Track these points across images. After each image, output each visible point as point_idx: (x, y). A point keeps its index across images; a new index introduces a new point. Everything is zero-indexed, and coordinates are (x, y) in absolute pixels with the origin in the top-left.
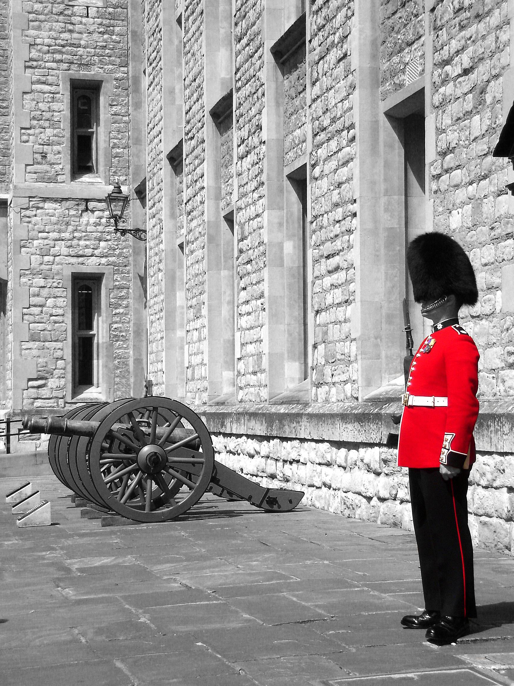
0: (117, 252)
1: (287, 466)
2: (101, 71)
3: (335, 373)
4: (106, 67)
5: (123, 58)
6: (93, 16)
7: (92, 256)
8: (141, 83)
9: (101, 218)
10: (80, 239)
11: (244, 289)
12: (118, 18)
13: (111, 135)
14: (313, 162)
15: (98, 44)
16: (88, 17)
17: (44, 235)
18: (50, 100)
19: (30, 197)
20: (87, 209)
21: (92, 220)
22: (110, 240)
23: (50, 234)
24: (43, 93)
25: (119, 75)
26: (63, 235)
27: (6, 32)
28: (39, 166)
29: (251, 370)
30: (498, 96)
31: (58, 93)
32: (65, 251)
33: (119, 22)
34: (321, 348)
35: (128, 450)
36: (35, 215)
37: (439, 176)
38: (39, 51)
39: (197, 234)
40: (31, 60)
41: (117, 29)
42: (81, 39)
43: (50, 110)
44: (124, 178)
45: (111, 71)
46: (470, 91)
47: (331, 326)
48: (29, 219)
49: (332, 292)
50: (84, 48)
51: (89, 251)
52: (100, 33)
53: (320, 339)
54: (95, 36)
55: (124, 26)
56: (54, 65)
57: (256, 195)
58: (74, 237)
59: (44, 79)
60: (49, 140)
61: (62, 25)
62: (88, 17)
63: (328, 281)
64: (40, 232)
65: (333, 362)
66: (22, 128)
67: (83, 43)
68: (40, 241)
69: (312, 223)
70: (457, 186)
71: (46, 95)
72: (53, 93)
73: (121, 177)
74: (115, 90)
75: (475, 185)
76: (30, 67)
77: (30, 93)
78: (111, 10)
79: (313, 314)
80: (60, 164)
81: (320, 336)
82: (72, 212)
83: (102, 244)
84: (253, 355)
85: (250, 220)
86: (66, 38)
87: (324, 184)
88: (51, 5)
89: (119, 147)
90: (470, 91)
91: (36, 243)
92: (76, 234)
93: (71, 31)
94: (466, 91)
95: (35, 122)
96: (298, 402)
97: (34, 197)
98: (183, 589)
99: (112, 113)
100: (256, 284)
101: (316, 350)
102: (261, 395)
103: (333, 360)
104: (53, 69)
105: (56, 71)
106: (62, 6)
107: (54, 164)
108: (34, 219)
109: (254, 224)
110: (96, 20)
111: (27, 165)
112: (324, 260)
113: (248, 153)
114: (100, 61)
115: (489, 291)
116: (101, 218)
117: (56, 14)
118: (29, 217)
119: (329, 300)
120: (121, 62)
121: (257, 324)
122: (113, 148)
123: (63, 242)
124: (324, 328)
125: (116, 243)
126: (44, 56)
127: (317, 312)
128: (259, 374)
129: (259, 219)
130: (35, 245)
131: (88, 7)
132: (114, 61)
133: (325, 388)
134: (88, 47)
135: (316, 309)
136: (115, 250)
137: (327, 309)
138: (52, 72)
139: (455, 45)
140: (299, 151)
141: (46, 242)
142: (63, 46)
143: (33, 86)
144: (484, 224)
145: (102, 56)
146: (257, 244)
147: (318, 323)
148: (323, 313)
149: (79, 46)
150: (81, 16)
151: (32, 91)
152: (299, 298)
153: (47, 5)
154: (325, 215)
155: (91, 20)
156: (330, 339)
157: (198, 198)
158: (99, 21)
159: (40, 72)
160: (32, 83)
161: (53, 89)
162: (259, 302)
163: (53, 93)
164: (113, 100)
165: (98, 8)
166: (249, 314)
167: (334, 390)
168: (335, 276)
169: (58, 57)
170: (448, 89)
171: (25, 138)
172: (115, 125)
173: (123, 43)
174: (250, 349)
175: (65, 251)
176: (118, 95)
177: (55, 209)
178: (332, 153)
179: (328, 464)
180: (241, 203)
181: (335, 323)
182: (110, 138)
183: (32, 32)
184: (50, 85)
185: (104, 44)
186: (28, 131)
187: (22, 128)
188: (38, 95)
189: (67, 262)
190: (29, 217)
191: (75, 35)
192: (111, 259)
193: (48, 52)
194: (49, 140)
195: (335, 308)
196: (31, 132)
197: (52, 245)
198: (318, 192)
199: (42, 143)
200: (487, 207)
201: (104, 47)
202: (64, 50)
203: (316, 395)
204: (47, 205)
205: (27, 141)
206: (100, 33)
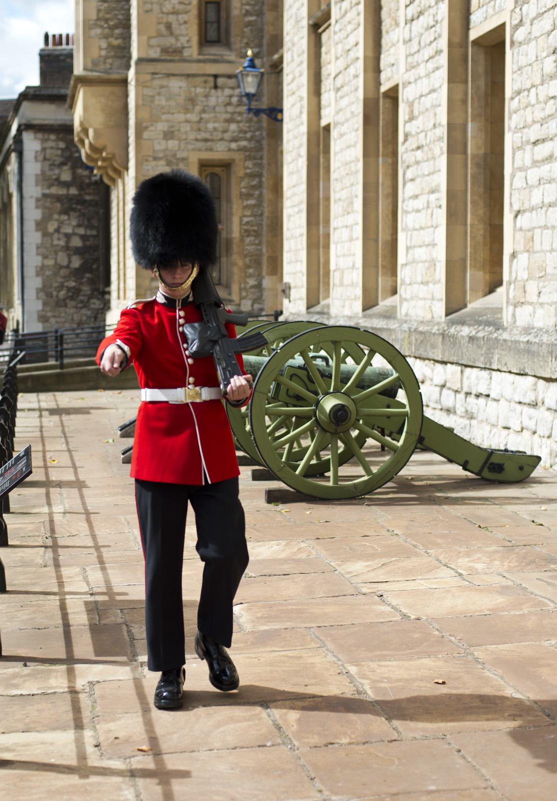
0: (249, 135)
1: (471, 399)
3: (543, 290)
9: (231, 96)
10: (207, 122)
11: (412, 180)
14: (515, 22)
20: (216, 87)
21: (221, 99)
23: (176, 115)
26: (188, 116)
29: (419, 279)
34: (523, 258)
35: (299, 399)
39: (348, 115)
47: (537, 232)
49: (542, 187)
53: (520, 247)
57: (431, 65)
63: (533, 175)
65: (542, 277)
69: (512, 99)
79: (512, 216)
81: (522, 243)
83: (233, 127)
84: (425, 262)
85: (421, 96)
87: (531, 50)
89: (251, 15)
96: (488, 323)
97: (156, 74)
98: (398, 618)
100: (428, 175)
101: (515, 261)
102: (434, 309)
103: (541, 275)
109: (427, 101)
112: (528, 148)
113: (421, 13)
119: (536, 198)
121: (429, 224)
124: (529, 234)
127: (518, 213)
128: (431, 285)
129: (434, 95)
133: (528, 309)
135: (516, 207)
136: (246, 132)
137: (532, 209)
140: (491, 11)
146: (431, 125)
147: (518, 226)
148: (527, 214)
152: (485, 193)
154: (533, 90)
156: (537, 247)
157: (352, 71)
162: (433, 197)
166: (418, 211)
167: (540, 312)
168: (546, 167)
174: (421, 253)
178: (544, 10)
179: (534, 405)
180: (411, 76)
181: (546, 227)
192: (244, 143)
195: (544, 209)
197: (176, 128)
198: (523, 61)
203: (514, 316)
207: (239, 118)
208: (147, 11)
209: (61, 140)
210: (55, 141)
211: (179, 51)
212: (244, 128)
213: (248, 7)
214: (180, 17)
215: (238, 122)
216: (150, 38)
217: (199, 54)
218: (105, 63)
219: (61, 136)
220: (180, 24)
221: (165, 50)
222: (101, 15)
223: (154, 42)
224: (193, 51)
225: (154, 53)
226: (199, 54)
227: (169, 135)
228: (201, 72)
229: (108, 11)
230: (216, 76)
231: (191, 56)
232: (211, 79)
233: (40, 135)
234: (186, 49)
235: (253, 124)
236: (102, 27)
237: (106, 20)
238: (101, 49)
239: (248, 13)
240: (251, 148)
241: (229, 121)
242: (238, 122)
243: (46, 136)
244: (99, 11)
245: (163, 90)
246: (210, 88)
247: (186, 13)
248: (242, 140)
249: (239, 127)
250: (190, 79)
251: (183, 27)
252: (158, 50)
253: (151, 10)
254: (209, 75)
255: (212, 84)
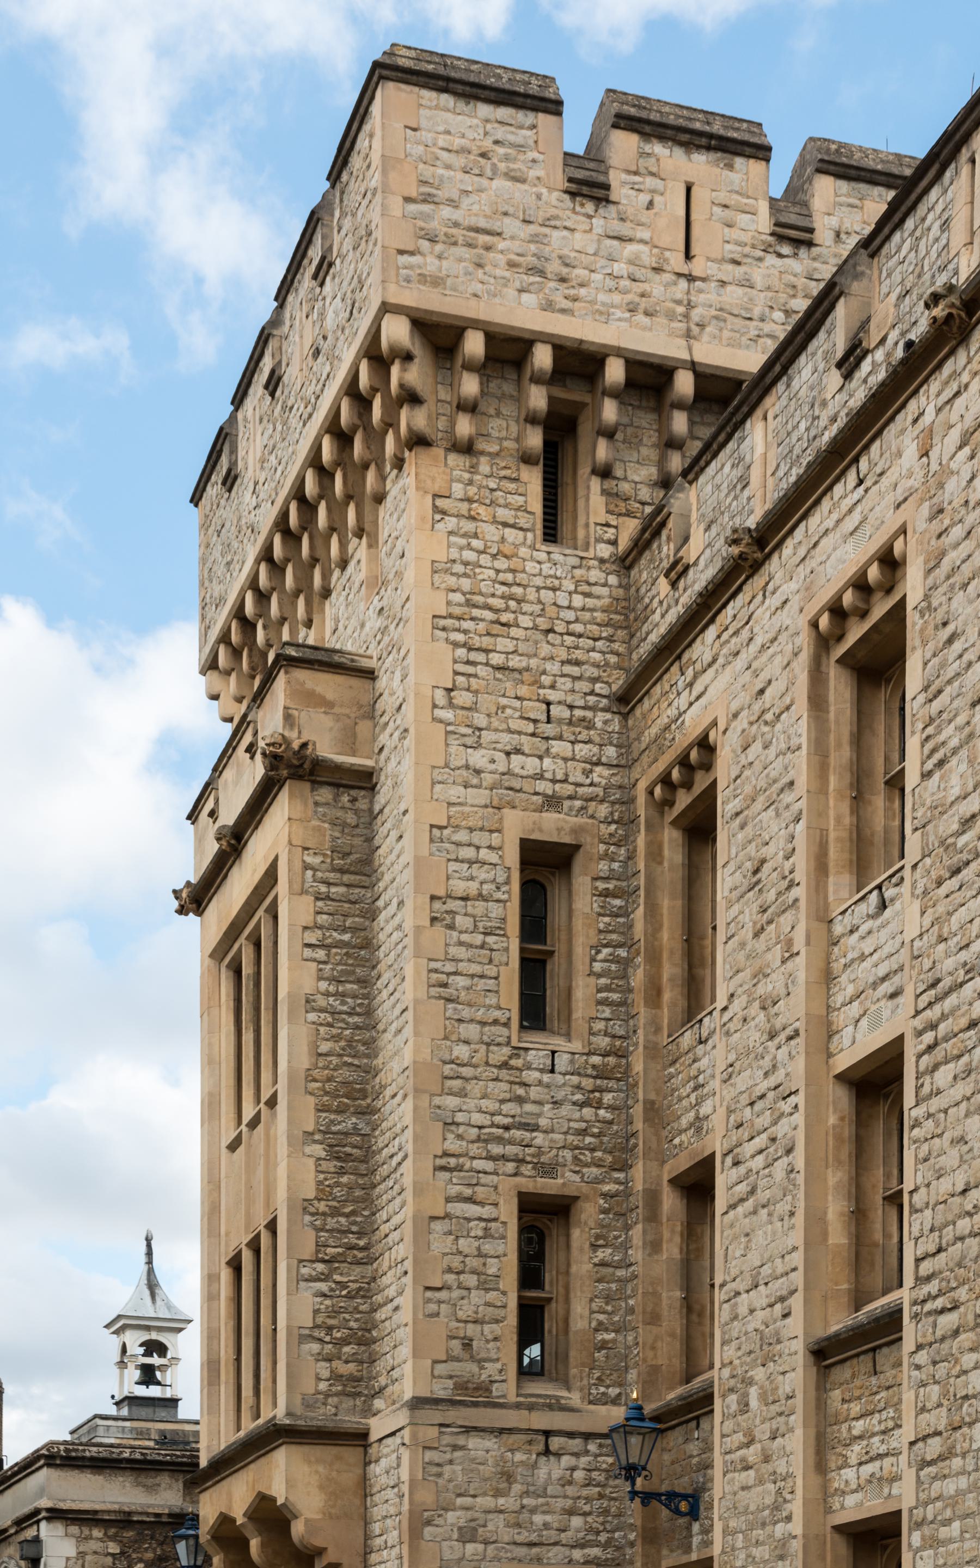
0: (603, 1537)
2: (577, 1178)
4: (585, 1170)
5: (617, 1154)
6: (563, 1069)
7: (556, 1544)
8: (661, 1203)
9: (573, 1469)
10: (533, 1511)
12: (610, 1075)
13: (594, 1305)
15: (572, 1124)
16: (552, 1071)
17: (467, 1501)
18: (480, 1233)
19: (441, 1425)
20: (547, 1452)
21: (556, 1474)
22: (590, 1514)
23: (478, 1500)
24: (465, 1218)
25: (608, 1188)
26: (501, 1501)
27: (369, 1101)
28: (456, 1364)
31: (495, 1220)
32: (506, 1535)
33: (612, 1084)
36: (451, 1462)
38: (460, 1137)
40: (446, 1154)
41: (608, 1098)
42: (539, 1115)
43: (480, 1254)
44: (617, 1391)
45: (597, 1181)
48: (439, 1469)
50: (545, 1132)
51: (552, 1535)
52: (574, 1104)
54: (566, 1110)
55: (621, 1091)
56: (489, 1166)
58: (523, 1507)
59: (468, 1192)
60: (476, 1313)
61: (504, 1086)
62: (552, 1071)
64: (459, 1495)
66: (428, 1288)
67: (543, 1122)
68: (459, 1513)
71: (472, 1224)
72: (485, 1220)
73: (610, 1390)
74: (602, 1216)
76: (443, 1168)
77: (443, 1218)
78: (596, 1060)
80: (498, 1360)
82: (519, 1457)
83: (576, 1522)
86: (512, 1113)
88: (484, 1047)
89: (606, 1330)
91: (451, 1516)
92: (525, 1501)
93: (520, 1100)
95: (451, 1278)
97: (448, 1426)
99: (596, 1260)
104: (485, 1173)
105: (491, 1177)
106: (506, 1051)
107: (486, 1360)
108: (447, 1469)
110: (568, 1077)
111: (435, 1362)
114: (575, 1158)
116: (573, 1469)
117: (495, 1066)
118: (438, 1465)
120: (614, 1163)
122: (596, 1330)
123: (502, 1516)
125: (601, 1519)
126: (470, 1146)
130: (449, 1521)
131: (553, 1052)
132: (600, 1159)
134: (552, 1131)
136: (598, 1533)
138: (484, 1179)
141: (469, 1514)
142: (507, 1128)
143: (449, 1205)
145: (577, 1148)
149: (535, 1128)
150: (542, 1071)
151: (448, 1216)
153: (477, 1047)
155: (559, 1079)
158: (575, 1079)
159: (464, 1177)
160: (448, 1200)
161: (486, 1212)
163: (485, 1220)
164: (598, 1237)
165: (573, 1054)
169: (496, 1149)
171: (433, 1307)
172: (601, 1286)
173: (618, 1124)
175: (506, 1535)
176: (607, 1226)
177: (487, 1451)
182: (592, 1312)
183: (451, 1102)
184: (481, 1204)
185: (584, 1125)
186: (438, 1295)
187: (428, 1288)
188: (459, 1223)
189: (509, 1555)
190: (438, 1465)
191: (528, 1107)
192: (595, 1552)
193: (478, 1140)
194: (476, 1313)
196: (443, 1295)
197: (481, 1522)
199: (464, 1318)
201: (583, 1132)
202: (507, 1135)
204: (474, 1442)
205: (438, 1314)
206: (574, 1104)
207: (587, 1508)
208: (432, 1315)
209: (112, 1538)
210: (101, 1540)
211: (485, 1388)
212: (594, 1525)
213: (602, 1317)
214: (487, 1328)
215: (585, 1514)
216: (435, 1362)
217: (518, 1396)
218: (325, 1404)
219: (112, 1531)
220: (488, 1341)
221: (462, 1386)
222: (319, 1320)
223: (440, 1369)
224: (508, 1389)
225: (442, 1389)
226: (518, 1396)
227: (468, 1535)
228: (524, 1426)
229: (334, 1312)
230: (547, 1434)
231: (504, 1396)
232: (541, 1438)
233: (74, 1529)
234: (495, 1385)
235: (610, 1518)
236: (321, 1340)
237: (330, 1329)
238: (319, 1379)
239: (601, 1327)
240: (607, 1560)
241: (571, 1512)
242: (585, 1514)
243: (86, 1531)
244: (316, 1312)
245: (458, 1454)
246: (538, 1454)
247: (497, 1321)
248: (592, 1546)
249: (586, 1522)
250: (505, 1436)
251: (491, 1345)
252: (450, 1383)
253: (438, 1314)
254: (537, 1431)
255: (541, 1447)
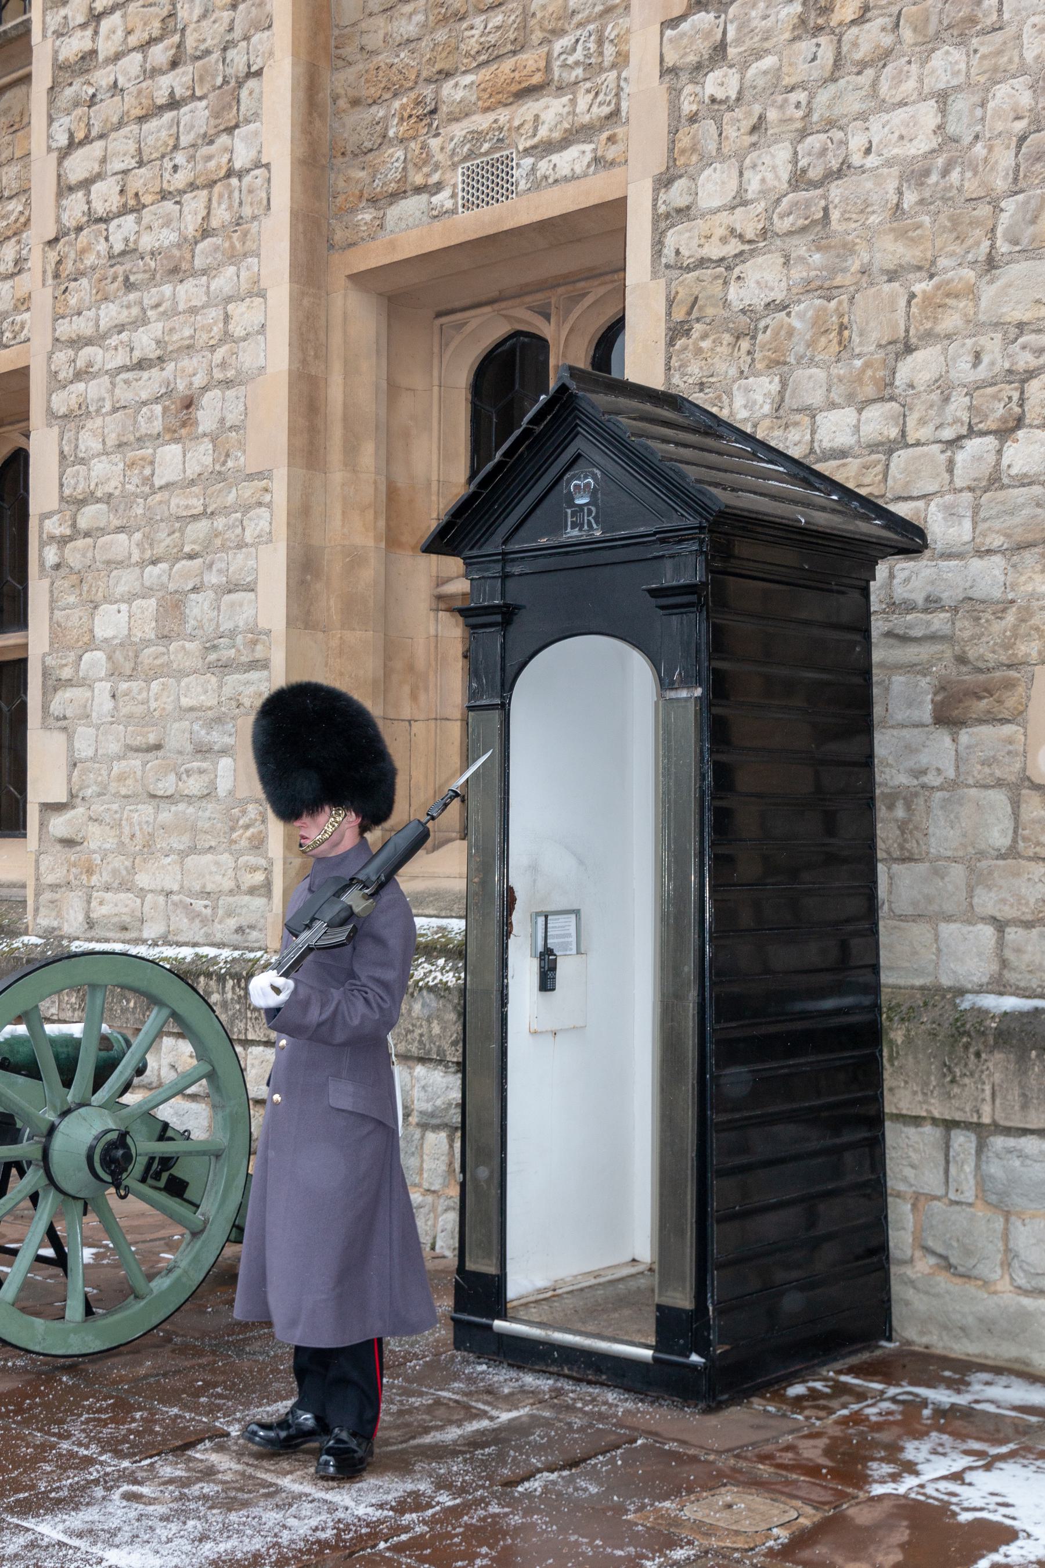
30: (231, 419)
37: (63, 541)
46: (157, 400)
70: (120, 564)
75: (163, 566)
90: (157, 400)
94: (144, 396)
115: (199, 756)
139: (110, 313)
144: (192, 638)
170: (94, 389)
200: (199, 607)
